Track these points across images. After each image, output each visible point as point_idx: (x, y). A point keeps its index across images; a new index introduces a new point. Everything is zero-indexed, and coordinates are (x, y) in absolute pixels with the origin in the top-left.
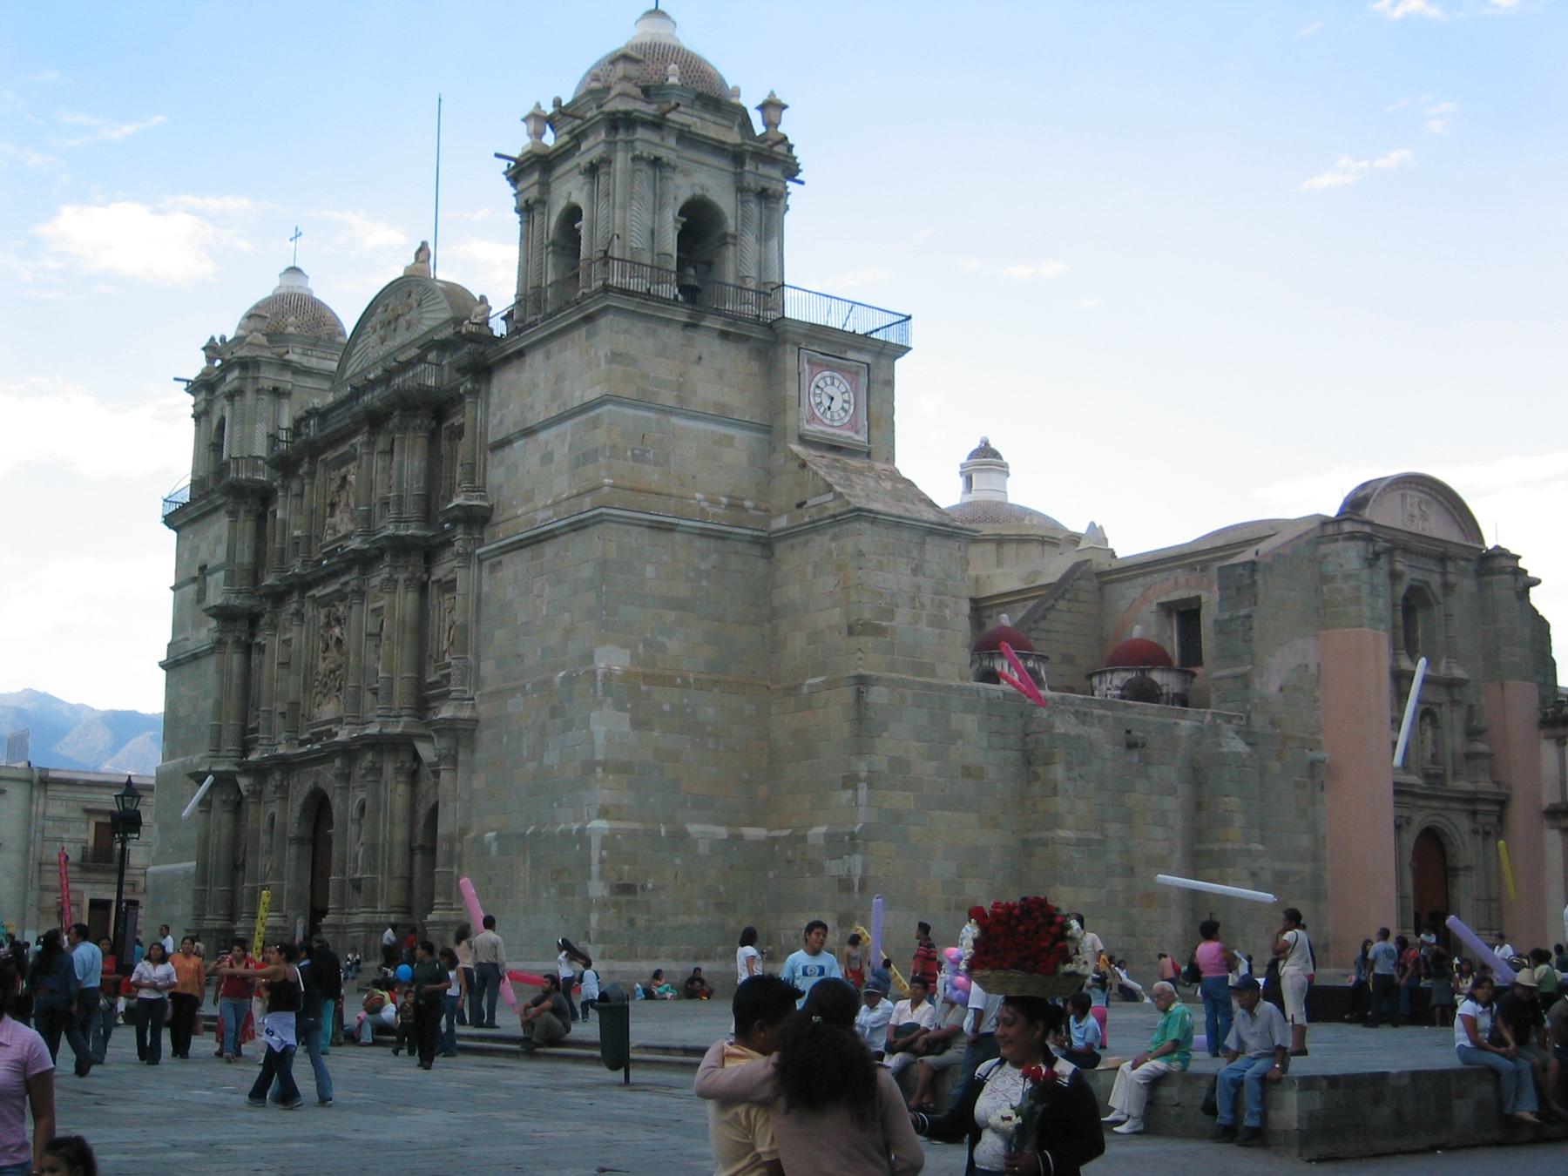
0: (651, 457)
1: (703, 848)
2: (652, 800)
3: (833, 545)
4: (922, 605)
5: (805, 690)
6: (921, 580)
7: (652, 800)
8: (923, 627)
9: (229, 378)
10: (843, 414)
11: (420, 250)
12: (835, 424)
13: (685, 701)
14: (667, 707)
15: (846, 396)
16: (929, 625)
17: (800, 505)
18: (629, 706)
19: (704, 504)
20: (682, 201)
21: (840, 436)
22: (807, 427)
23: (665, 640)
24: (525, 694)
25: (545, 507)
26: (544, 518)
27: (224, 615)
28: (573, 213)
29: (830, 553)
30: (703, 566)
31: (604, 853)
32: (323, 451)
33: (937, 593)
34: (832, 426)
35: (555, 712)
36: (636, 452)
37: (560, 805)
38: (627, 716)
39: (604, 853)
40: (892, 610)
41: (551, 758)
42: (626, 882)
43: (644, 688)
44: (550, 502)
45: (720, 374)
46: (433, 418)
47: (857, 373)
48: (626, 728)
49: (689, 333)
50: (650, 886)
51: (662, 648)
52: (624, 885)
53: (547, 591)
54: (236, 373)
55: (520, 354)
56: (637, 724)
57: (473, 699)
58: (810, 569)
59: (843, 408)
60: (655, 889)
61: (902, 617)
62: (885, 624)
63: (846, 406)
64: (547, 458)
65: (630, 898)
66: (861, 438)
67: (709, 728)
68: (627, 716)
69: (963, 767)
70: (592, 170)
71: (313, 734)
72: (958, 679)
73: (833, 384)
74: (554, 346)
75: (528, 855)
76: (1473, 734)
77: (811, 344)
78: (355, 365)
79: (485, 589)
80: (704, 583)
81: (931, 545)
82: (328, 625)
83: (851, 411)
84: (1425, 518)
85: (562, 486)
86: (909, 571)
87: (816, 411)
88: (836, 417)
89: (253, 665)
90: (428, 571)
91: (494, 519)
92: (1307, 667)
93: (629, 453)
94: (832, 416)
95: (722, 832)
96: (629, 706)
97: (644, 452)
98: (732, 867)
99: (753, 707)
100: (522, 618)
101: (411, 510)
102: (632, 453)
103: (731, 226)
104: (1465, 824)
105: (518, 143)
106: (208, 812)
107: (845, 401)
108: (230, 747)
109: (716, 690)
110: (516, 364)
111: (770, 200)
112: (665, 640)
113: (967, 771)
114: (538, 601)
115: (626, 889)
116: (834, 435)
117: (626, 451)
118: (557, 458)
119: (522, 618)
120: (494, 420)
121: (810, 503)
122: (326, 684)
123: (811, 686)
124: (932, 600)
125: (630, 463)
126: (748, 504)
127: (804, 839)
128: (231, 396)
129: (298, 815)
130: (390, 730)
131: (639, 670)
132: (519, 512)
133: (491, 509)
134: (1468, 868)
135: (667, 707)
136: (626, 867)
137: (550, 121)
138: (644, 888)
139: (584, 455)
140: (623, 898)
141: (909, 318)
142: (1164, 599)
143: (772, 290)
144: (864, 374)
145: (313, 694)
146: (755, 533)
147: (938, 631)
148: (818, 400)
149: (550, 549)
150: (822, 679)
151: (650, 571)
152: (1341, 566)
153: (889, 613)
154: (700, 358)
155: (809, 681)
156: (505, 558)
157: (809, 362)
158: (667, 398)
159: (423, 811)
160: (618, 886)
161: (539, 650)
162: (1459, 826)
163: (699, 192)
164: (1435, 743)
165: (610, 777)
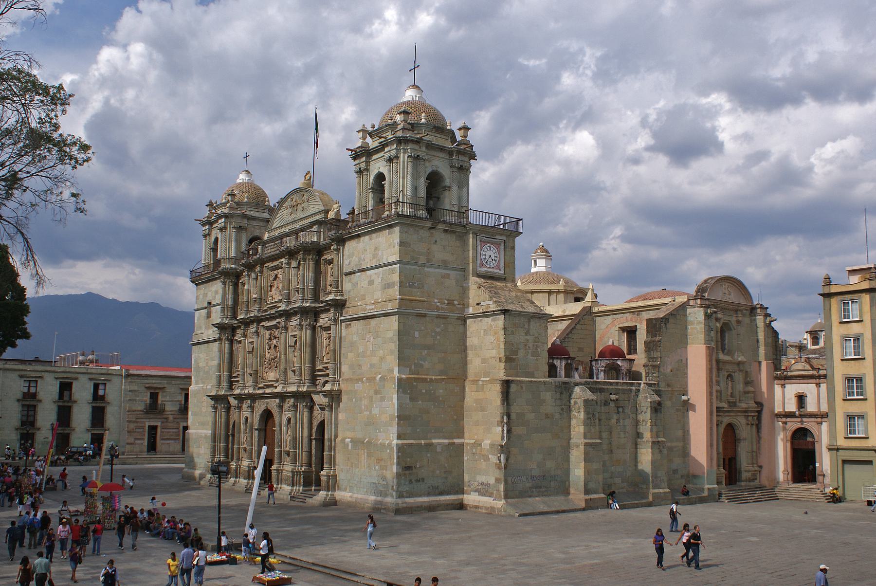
1: (439, 449)
2: (418, 430)
3: (493, 323)
4: (529, 347)
5: (481, 383)
6: (528, 337)
7: (418, 430)
8: (529, 356)
9: (220, 221)
11: (307, 174)
13: (431, 388)
14: (424, 391)
15: (496, 255)
16: (531, 356)
17: (478, 304)
19: (438, 304)
20: (428, 173)
22: (481, 269)
23: (423, 363)
24: (363, 382)
25: (371, 304)
26: (371, 310)
27: (221, 327)
28: (380, 177)
29: (491, 326)
30: (438, 330)
31: (400, 454)
32: (267, 262)
33: (535, 342)
35: (377, 392)
36: (411, 283)
37: (380, 432)
38: (408, 396)
39: (400, 454)
41: (375, 411)
42: (408, 465)
43: (415, 384)
44: (373, 302)
45: (444, 247)
46: (317, 255)
47: (500, 244)
48: (408, 401)
49: (431, 231)
50: (418, 466)
51: (422, 366)
52: (408, 467)
53: (372, 339)
54: (223, 220)
55: (358, 236)
56: (412, 399)
57: (339, 381)
58: (482, 331)
60: (419, 467)
61: (521, 353)
62: (514, 357)
63: (496, 258)
64: (371, 283)
65: (411, 472)
66: (502, 272)
68: (408, 396)
69: (546, 414)
70: (390, 160)
71: (265, 385)
74: (374, 235)
75: (366, 451)
76: (747, 383)
77: (482, 234)
78: (278, 222)
79: (343, 334)
80: (438, 337)
82: (270, 339)
83: (498, 261)
84: (730, 294)
85: (378, 295)
86: (524, 334)
87: (483, 262)
89: (234, 349)
90: (316, 321)
91: (347, 305)
92: (682, 360)
93: (408, 284)
94: (490, 263)
95: (446, 441)
96: (409, 391)
97: (413, 283)
98: (450, 456)
99: (458, 388)
100: (361, 350)
101: (309, 295)
103: (447, 182)
104: (743, 421)
105: (357, 143)
106: (216, 412)
107: (495, 257)
108: (225, 384)
109: (443, 383)
110: (356, 240)
111: (464, 171)
112: (423, 363)
113: (547, 416)
114: (368, 343)
115: (408, 468)
116: (491, 272)
117: (406, 284)
118: (376, 283)
119: (361, 350)
120: (346, 262)
121: (482, 304)
122: (270, 364)
123: (483, 381)
124: (533, 345)
126: (456, 302)
127: (481, 445)
128: (221, 229)
129: (259, 419)
130: (300, 389)
131: (413, 376)
132: (359, 304)
133: (345, 301)
134: (745, 439)
136: (409, 459)
137: (371, 135)
138: (415, 467)
139: (388, 284)
140: (407, 472)
141: (522, 219)
142: (621, 325)
143: (463, 211)
144: (502, 244)
145: (264, 368)
146: (459, 315)
147: (535, 358)
148: (484, 257)
149: (373, 322)
150: (488, 379)
151: (417, 334)
152: (697, 318)
154: (436, 241)
155: (482, 379)
156: (353, 323)
157: (480, 241)
158: (423, 260)
159: (315, 424)
160: (405, 467)
161: (369, 364)
162: (741, 422)
163: (435, 169)
164: (732, 388)
165: (402, 422)
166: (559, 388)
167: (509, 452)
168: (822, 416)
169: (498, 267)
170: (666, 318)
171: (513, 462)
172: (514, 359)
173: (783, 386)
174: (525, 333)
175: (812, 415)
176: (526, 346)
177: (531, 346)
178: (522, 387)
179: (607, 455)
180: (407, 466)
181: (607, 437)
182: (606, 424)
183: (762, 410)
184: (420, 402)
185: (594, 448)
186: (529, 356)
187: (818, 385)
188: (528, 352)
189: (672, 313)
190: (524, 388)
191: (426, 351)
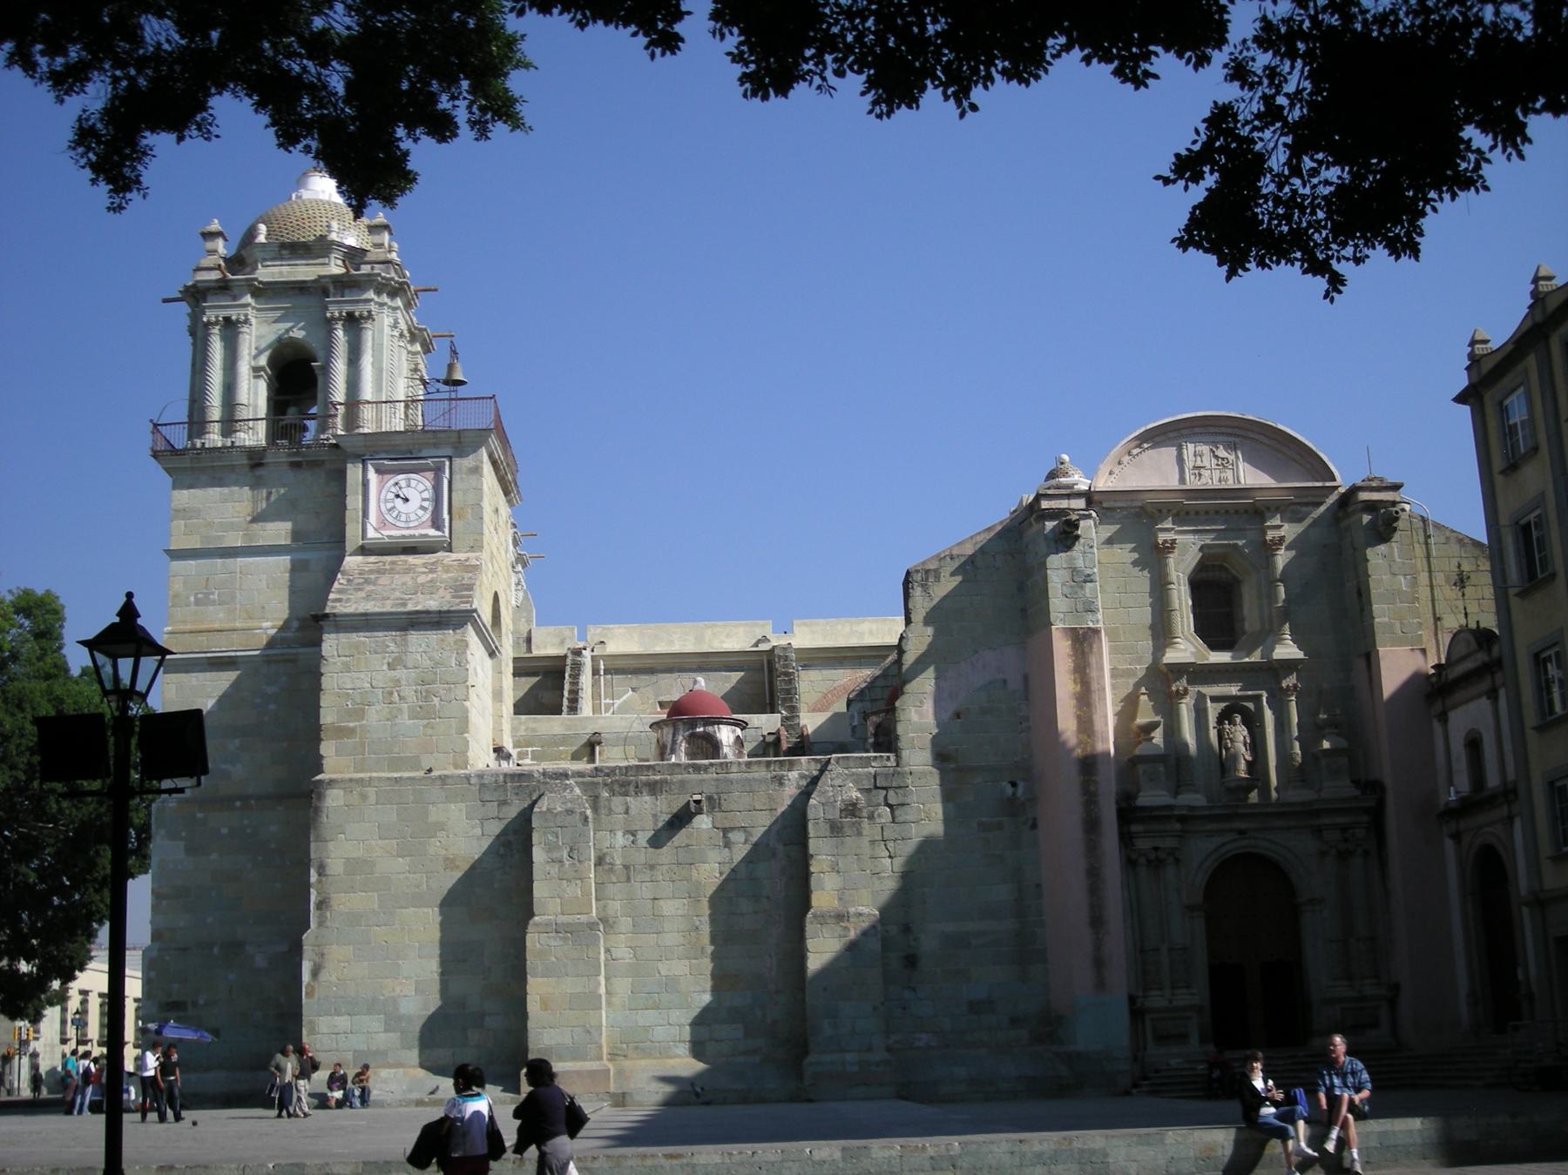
0: (216, 597)
2: (210, 920)
6: (400, 673)
7: (210, 920)
8: (405, 720)
10: (421, 512)
12: (412, 525)
14: (225, 831)
16: (409, 719)
18: (183, 834)
21: (413, 536)
31: (152, 974)
34: (408, 528)
36: (200, 596)
40: (363, 710)
43: (200, 815)
50: (201, 1002)
59: (422, 508)
62: (351, 725)
65: (182, 1014)
67: (273, 846)
68: (181, 844)
72: (452, 767)
73: (409, 486)
77: (377, 453)
80: (272, 707)
81: (416, 638)
86: (385, 667)
87: (388, 517)
88: (413, 517)
92: (1005, 682)
93: (192, 599)
96: (183, 834)
97: (207, 595)
102: (196, 598)
125: (193, 608)
135: (225, 831)
138: (195, 1004)
148: (390, 505)
153: (359, 713)
160: (167, 1004)
166: (495, 790)
167: (323, 955)
168: (1508, 794)
169: (383, 523)
170: (927, 572)
171: (334, 979)
172: (352, 731)
173: (1443, 718)
174: (389, 664)
175: (1492, 800)
176: (391, 694)
177: (409, 692)
178: (364, 797)
179: (687, 962)
180: (171, 1000)
181: (680, 912)
182: (675, 877)
183: (1381, 803)
184: (214, 857)
185: (565, 939)
186: (405, 720)
187: (1493, 694)
188: (400, 710)
189: (954, 552)
190: (372, 798)
191: (237, 742)
